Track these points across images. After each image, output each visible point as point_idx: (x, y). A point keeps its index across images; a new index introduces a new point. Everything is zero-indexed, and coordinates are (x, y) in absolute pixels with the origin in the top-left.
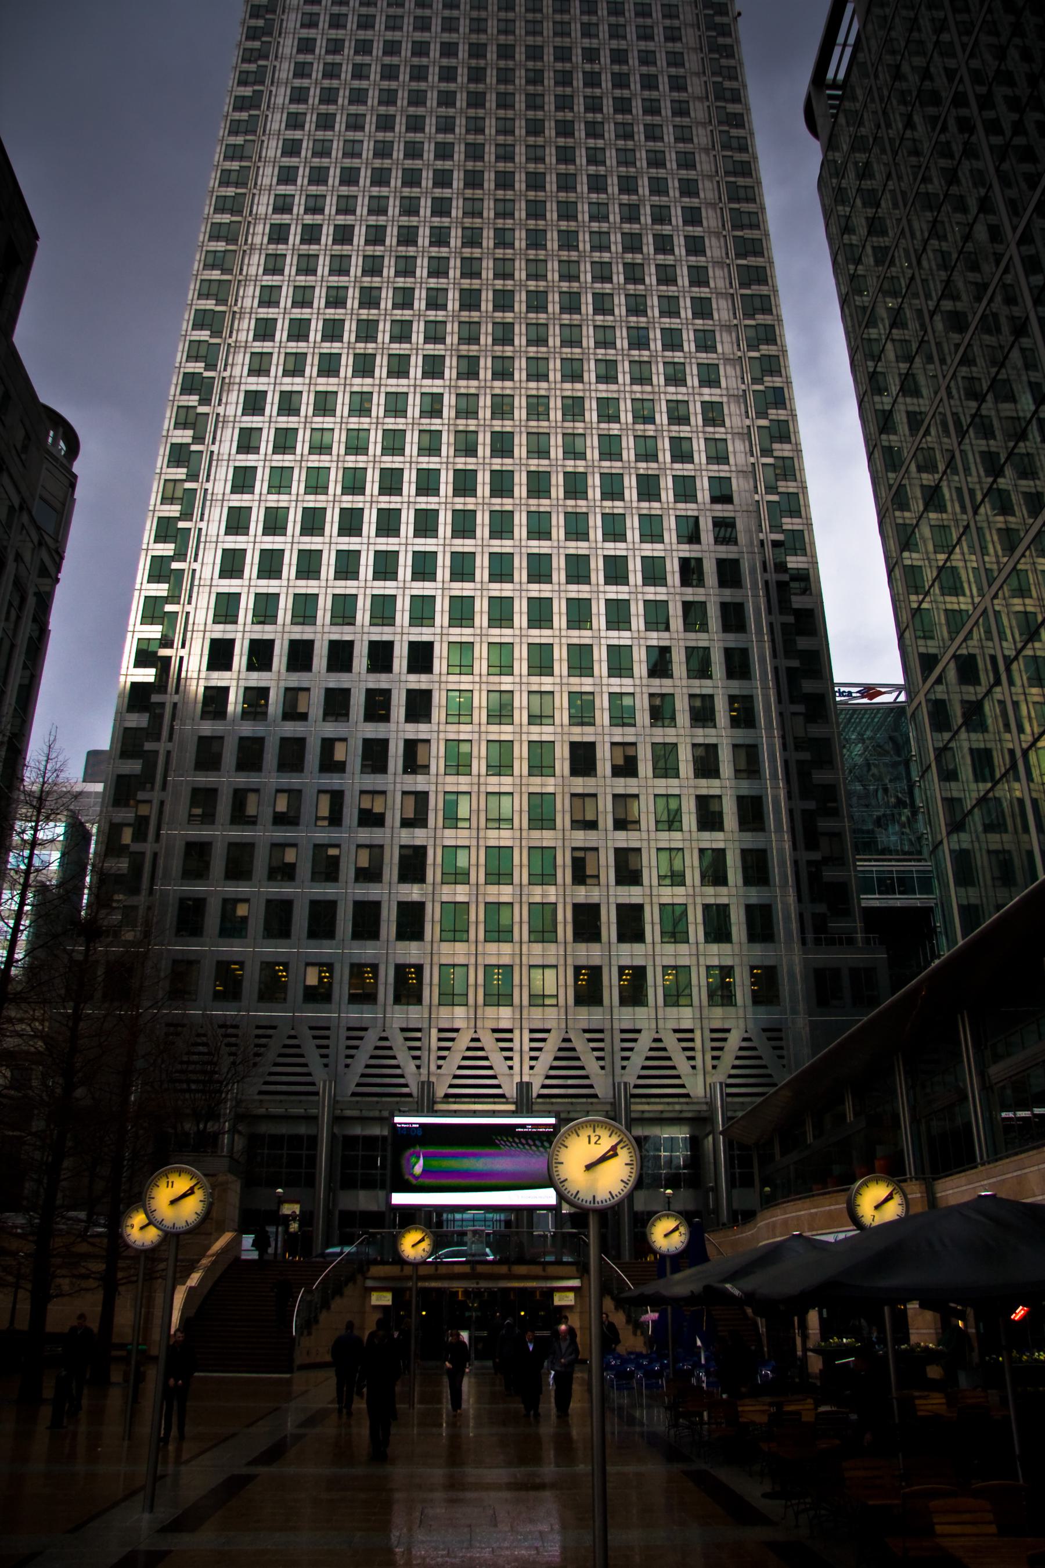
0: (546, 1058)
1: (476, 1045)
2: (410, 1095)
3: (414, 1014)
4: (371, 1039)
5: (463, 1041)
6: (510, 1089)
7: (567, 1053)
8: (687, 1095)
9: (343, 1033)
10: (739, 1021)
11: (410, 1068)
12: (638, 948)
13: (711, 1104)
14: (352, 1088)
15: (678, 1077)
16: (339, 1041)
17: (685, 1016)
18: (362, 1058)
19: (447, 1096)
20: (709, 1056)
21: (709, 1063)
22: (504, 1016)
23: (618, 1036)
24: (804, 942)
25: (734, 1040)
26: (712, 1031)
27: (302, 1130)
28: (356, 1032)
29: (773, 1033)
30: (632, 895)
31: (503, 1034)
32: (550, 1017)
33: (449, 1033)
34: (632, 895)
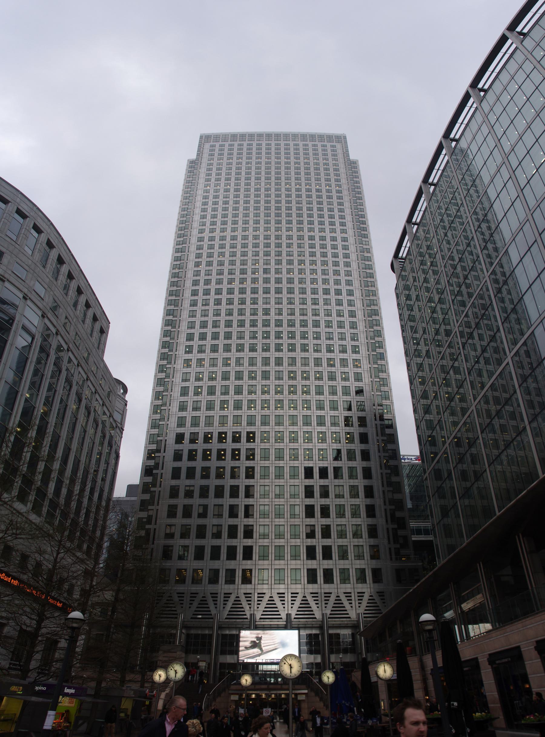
0: (297, 603)
1: (271, 599)
2: (247, 618)
3: (248, 588)
4: (233, 598)
7: (305, 600)
8: (349, 618)
9: (223, 595)
10: (368, 588)
11: (247, 608)
12: (330, 562)
13: (358, 621)
14: (225, 616)
15: (346, 610)
16: (221, 598)
17: (348, 588)
18: (229, 605)
19: (261, 618)
21: (357, 605)
23: (323, 595)
24: (391, 559)
25: (366, 597)
26: (358, 593)
27: (207, 632)
28: (227, 595)
29: (381, 594)
30: (327, 542)
31: (281, 595)
32: (298, 588)
33: (261, 595)
34: (327, 542)
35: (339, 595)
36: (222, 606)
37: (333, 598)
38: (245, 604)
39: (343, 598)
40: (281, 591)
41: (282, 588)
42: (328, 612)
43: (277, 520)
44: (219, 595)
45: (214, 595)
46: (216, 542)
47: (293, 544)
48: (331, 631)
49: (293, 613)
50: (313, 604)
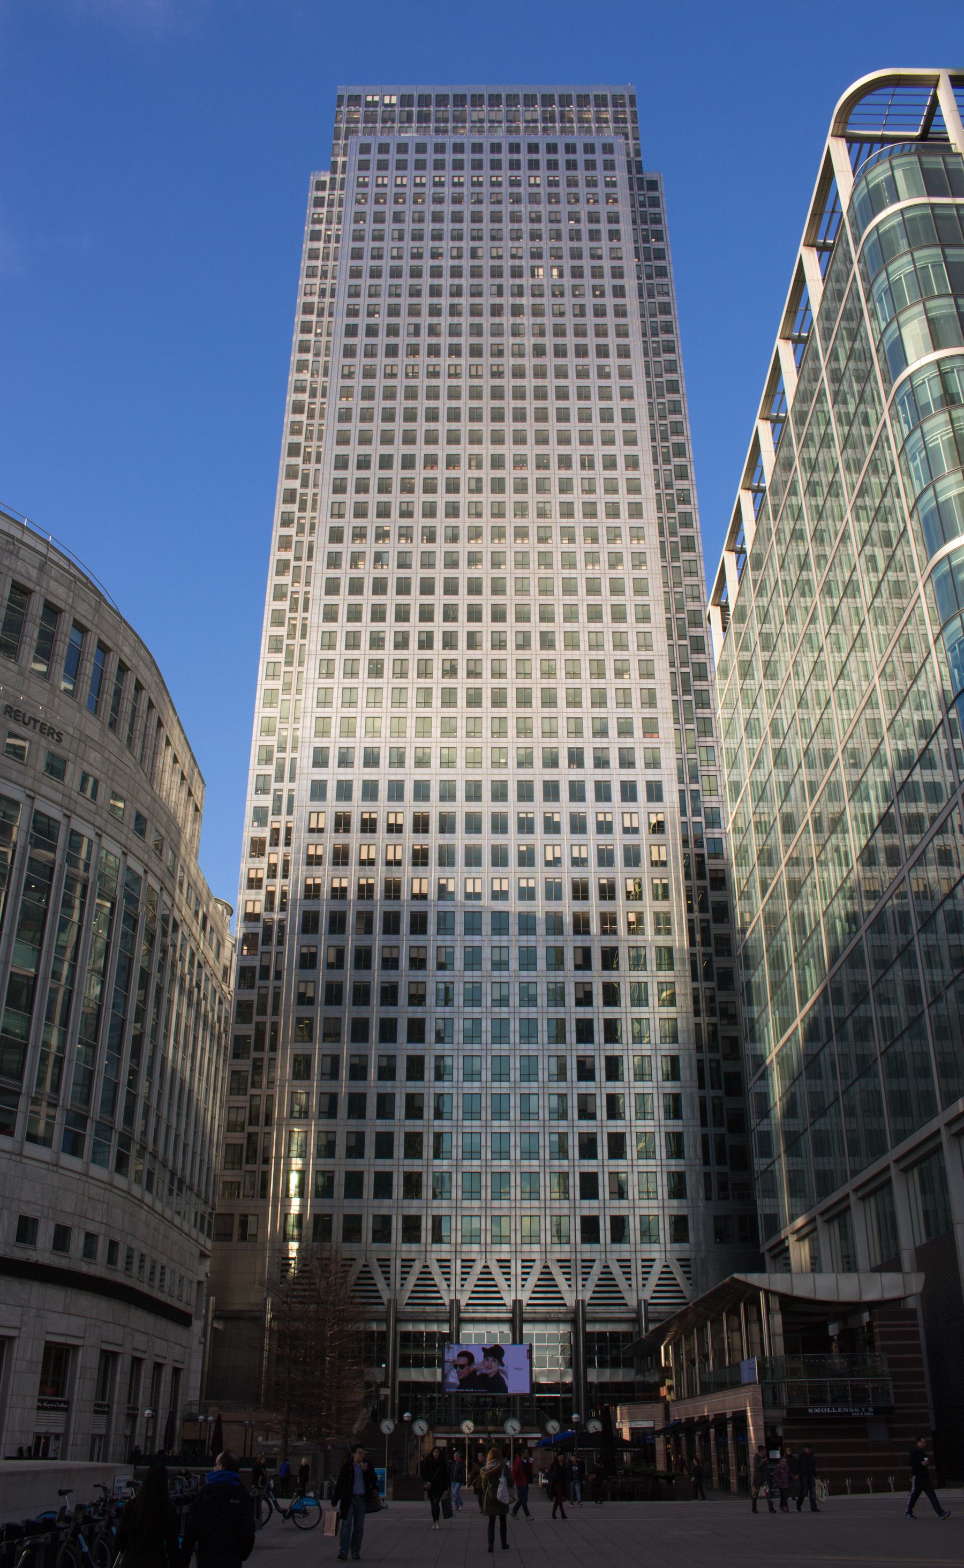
0: (533, 1279)
1: (486, 1271)
4: (417, 1267)
5: (478, 1267)
6: (508, 1299)
7: (546, 1273)
11: (443, 1285)
12: (594, 1203)
13: (638, 1312)
14: (406, 1300)
16: (396, 1267)
20: (640, 1277)
21: (640, 1282)
22: (505, 1250)
23: (579, 1264)
25: (657, 1268)
28: (407, 1263)
31: (504, 1264)
33: (468, 1263)
35: (610, 1263)
36: (399, 1282)
37: (597, 1269)
38: (438, 1279)
39: (616, 1270)
40: (504, 1257)
41: (505, 1250)
42: (587, 1295)
43: (496, 1123)
44: (392, 1263)
45: (385, 1263)
46: (383, 1165)
47: (526, 1169)
48: (590, 1328)
49: (525, 1296)
50: (560, 1280)
